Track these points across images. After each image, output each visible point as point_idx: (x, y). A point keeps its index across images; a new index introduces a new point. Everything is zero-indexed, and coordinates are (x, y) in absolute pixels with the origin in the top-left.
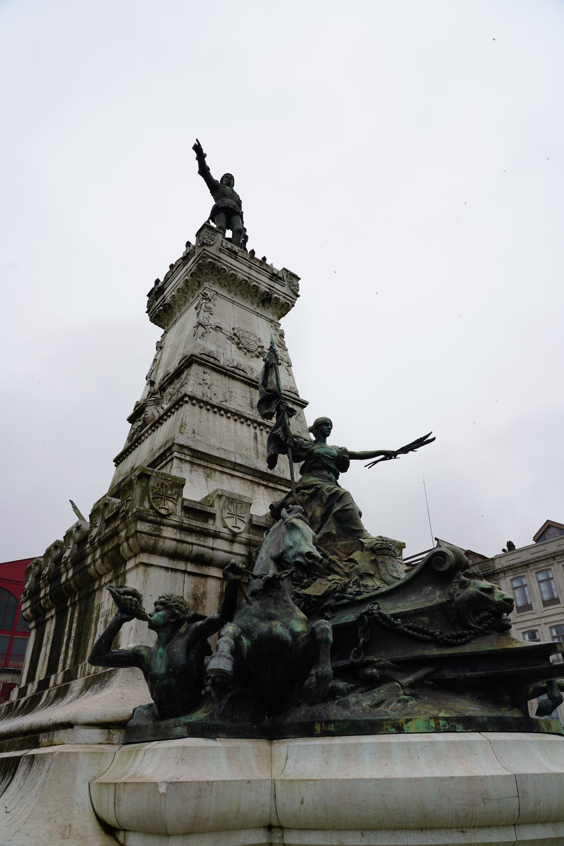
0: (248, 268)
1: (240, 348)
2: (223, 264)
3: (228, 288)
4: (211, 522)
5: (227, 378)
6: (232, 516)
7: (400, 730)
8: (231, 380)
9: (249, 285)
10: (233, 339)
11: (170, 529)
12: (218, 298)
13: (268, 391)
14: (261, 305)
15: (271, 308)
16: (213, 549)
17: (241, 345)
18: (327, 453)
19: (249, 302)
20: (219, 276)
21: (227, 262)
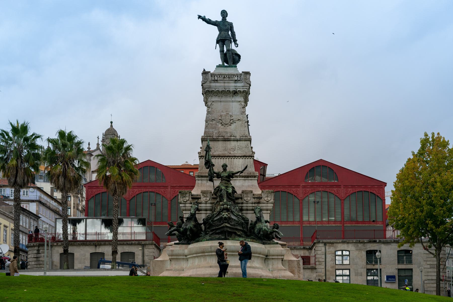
0: (223, 84)
1: (222, 125)
2: (212, 88)
3: (218, 96)
4: (200, 200)
5: (216, 142)
6: (205, 197)
7: (201, 241)
8: (218, 142)
9: (225, 91)
10: (220, 122)
11: (188, 204)
12: (213, 103)
13: (206, 161)
14: (234, 95)
15: (239, 95)
16: (201, 207)
17: (223, 123)
18: (224, 175)
19: (229, 97)
20: (213, 93)
21: (214, 86)
